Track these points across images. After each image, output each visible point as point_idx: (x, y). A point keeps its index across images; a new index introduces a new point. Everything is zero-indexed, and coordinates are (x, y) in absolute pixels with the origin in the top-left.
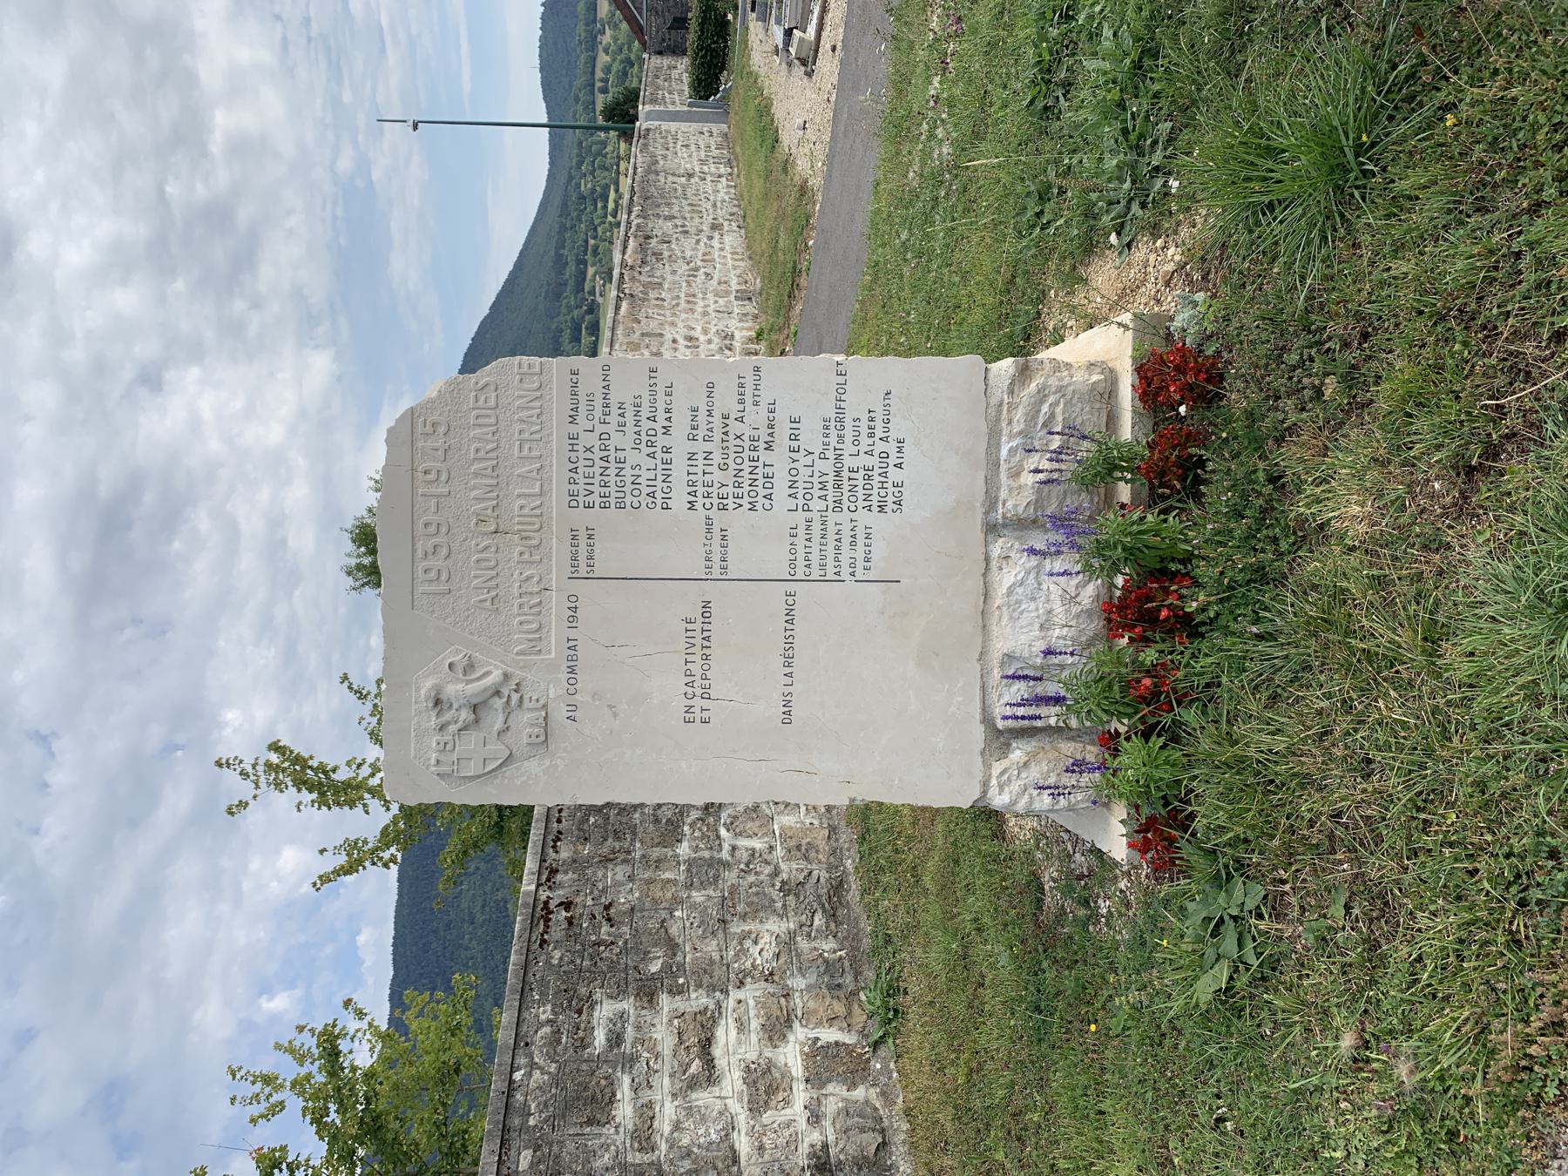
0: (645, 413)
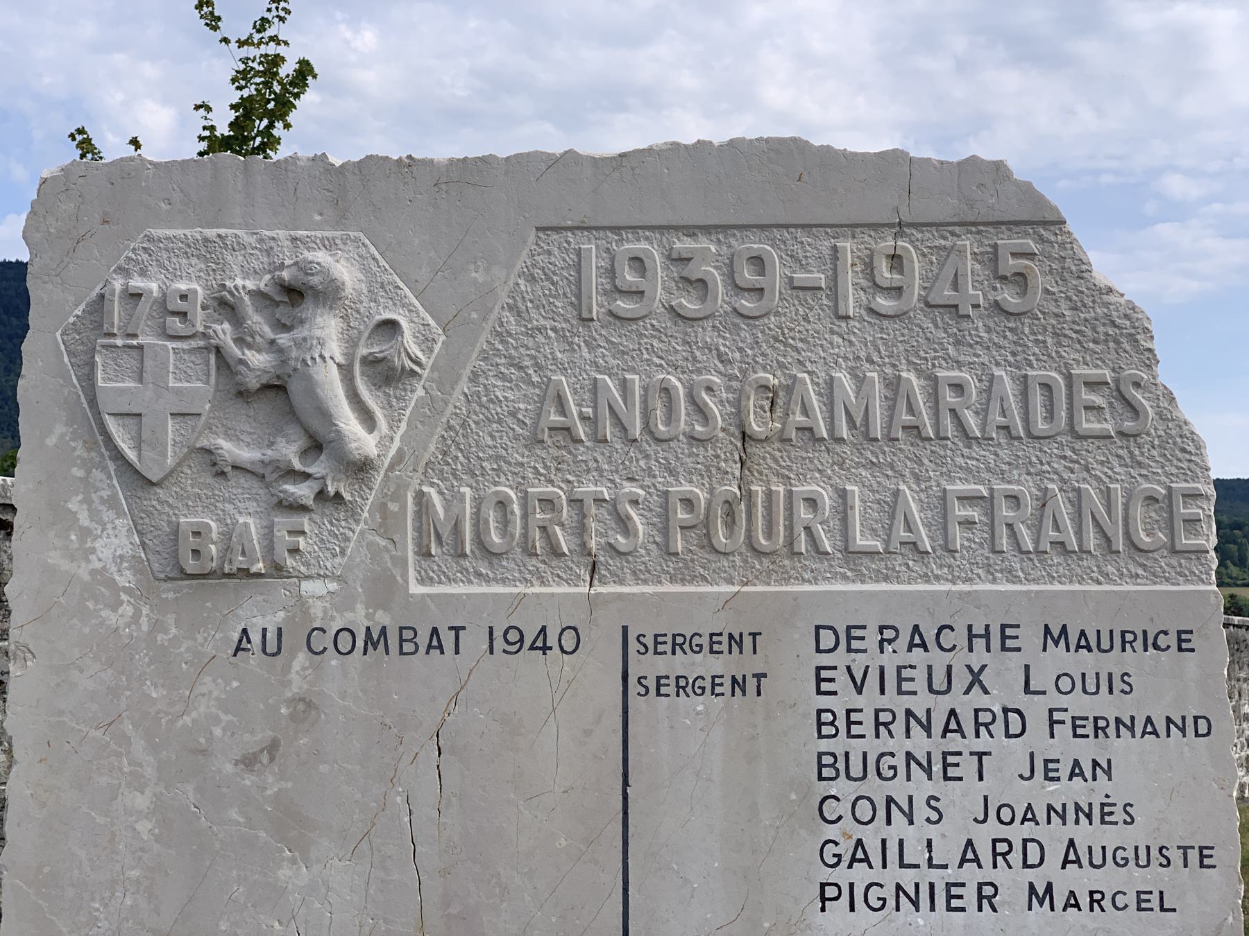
0: (1086, 834)
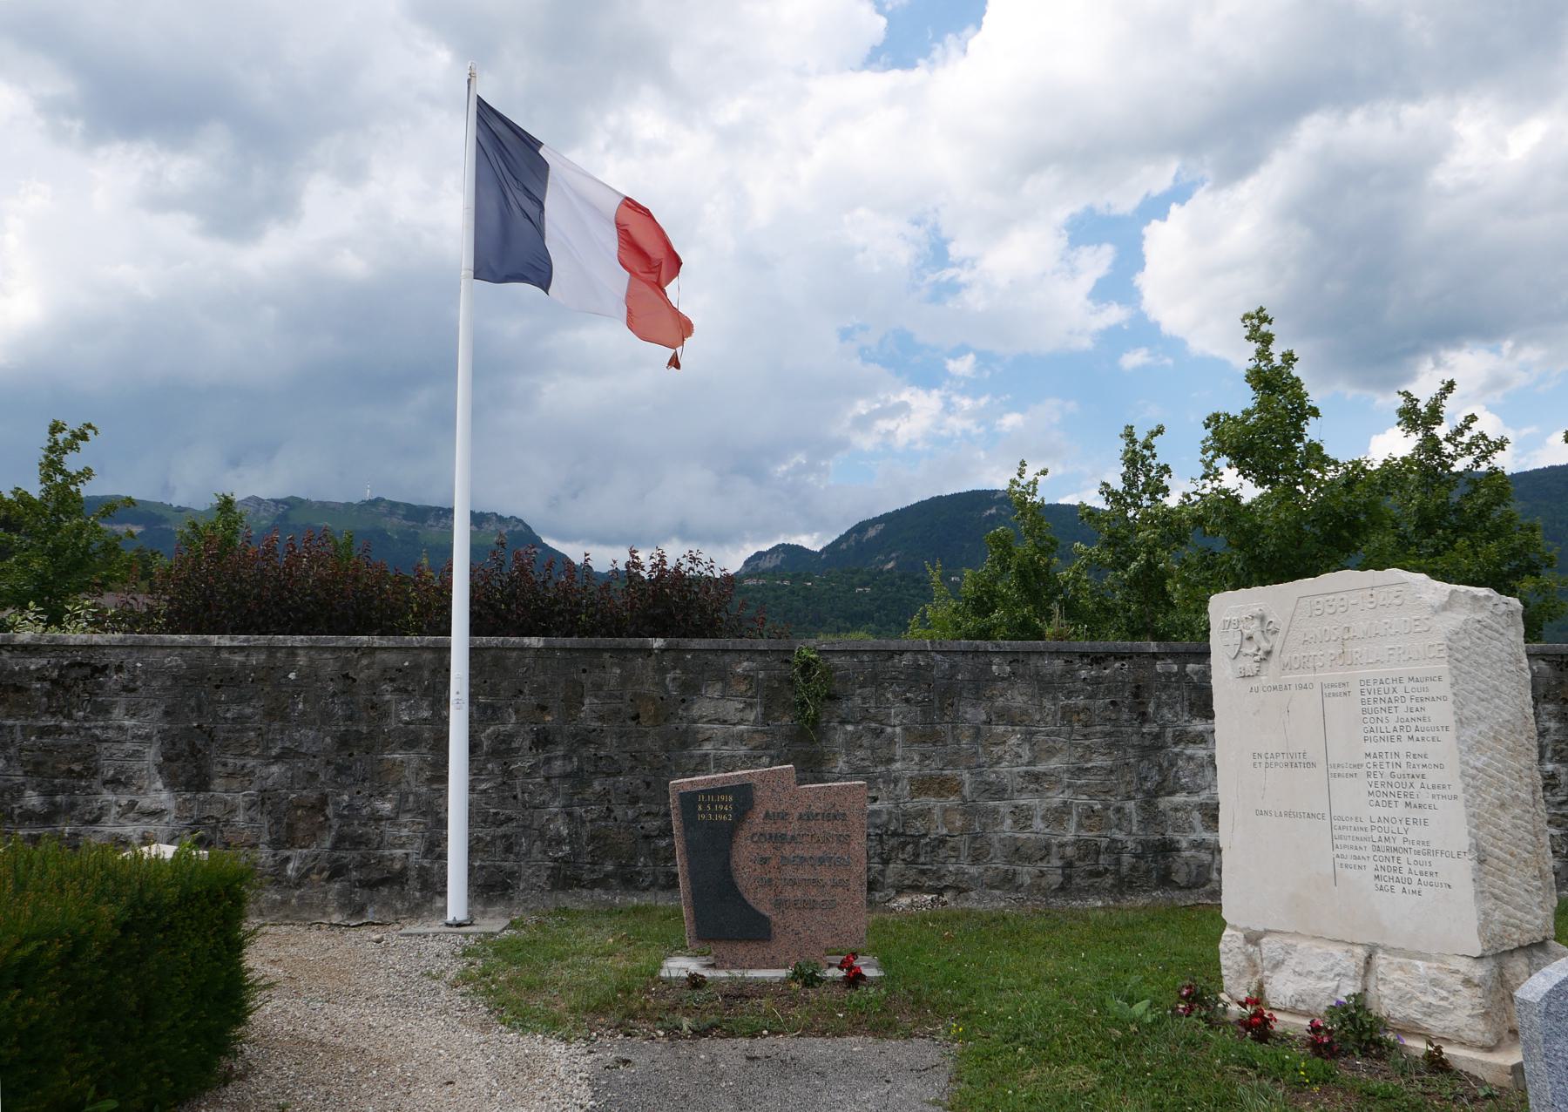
0: (1420, 724)
